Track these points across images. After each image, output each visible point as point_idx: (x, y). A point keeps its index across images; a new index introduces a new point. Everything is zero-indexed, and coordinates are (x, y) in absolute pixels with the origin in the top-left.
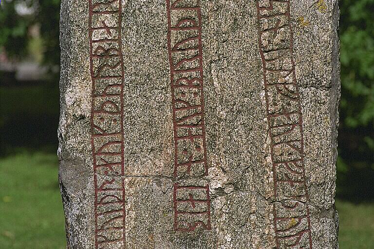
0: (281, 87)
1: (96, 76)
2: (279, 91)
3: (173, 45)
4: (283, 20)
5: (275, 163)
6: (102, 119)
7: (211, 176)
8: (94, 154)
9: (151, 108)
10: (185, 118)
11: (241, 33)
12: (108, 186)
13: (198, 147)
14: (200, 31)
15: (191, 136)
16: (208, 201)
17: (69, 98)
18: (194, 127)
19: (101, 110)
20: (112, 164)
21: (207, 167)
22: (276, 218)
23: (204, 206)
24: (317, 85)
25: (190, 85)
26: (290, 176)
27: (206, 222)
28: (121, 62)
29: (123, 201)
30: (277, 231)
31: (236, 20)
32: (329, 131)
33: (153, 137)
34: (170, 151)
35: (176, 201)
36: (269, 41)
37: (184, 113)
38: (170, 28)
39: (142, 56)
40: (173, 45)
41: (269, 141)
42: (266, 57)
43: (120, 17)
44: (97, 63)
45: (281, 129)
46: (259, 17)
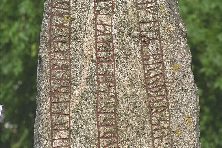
4: (166, 132)
11: (142, 140)
14: (117, 139)
31: (138, 132)
36: (159, 145)
43: (70, 132)
46: (152, 130)
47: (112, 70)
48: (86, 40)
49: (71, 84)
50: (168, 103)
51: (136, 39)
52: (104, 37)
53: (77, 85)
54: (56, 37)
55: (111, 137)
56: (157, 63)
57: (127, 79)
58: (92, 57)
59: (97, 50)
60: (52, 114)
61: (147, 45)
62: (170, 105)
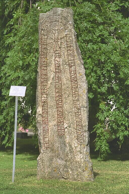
0: (77, 108)
2: (77, 108)
3: (57, 100)
4: (77, 95)
5: (76, 122)
6: (44, 114)
7: (64, 125)
8: (43, 121)
9: (53, 112)
10: (59, 114)
11: (69, 98)
12: (45, 127)
13: (62, 119)
14: (62, 97)
15: (61, 117)
16: (64, 130)
17: (38, 111)
18: (61, 115)
19: (44, 113)
20: (46, 123)
21: (64, 123)
22: (77, 133)
23: (63, 130)
24: (84, 107)
25: (60, 108)
26: (79, 124)
27: (64, 134)
28: (47, 103)
29: (48, 130)
30: (77, 135)
31: (68, 95)
32: (86, 116)
33: (54, 117)
34: (57, 120)
35: (58, 130)
37: (59, 113)
39: (51, 102)
40: (57, 100)
41: (75, 118)
42: (74, 102)
43: (47, 95)
44: (43, 104)
45: (77, 116)
46: (73, 95)
47: (60, 76)
48: (52, 66)
50: (78, 86)
51: (68, 66)
52: (58, 65)
53: (49, 80)
54: (43, 65)
55: (60, 97)
56: (74, 73)
57: (65, 78)
59: (56, 69)
60: (41, 89)
61: (71, 67)
62: (78, 87)
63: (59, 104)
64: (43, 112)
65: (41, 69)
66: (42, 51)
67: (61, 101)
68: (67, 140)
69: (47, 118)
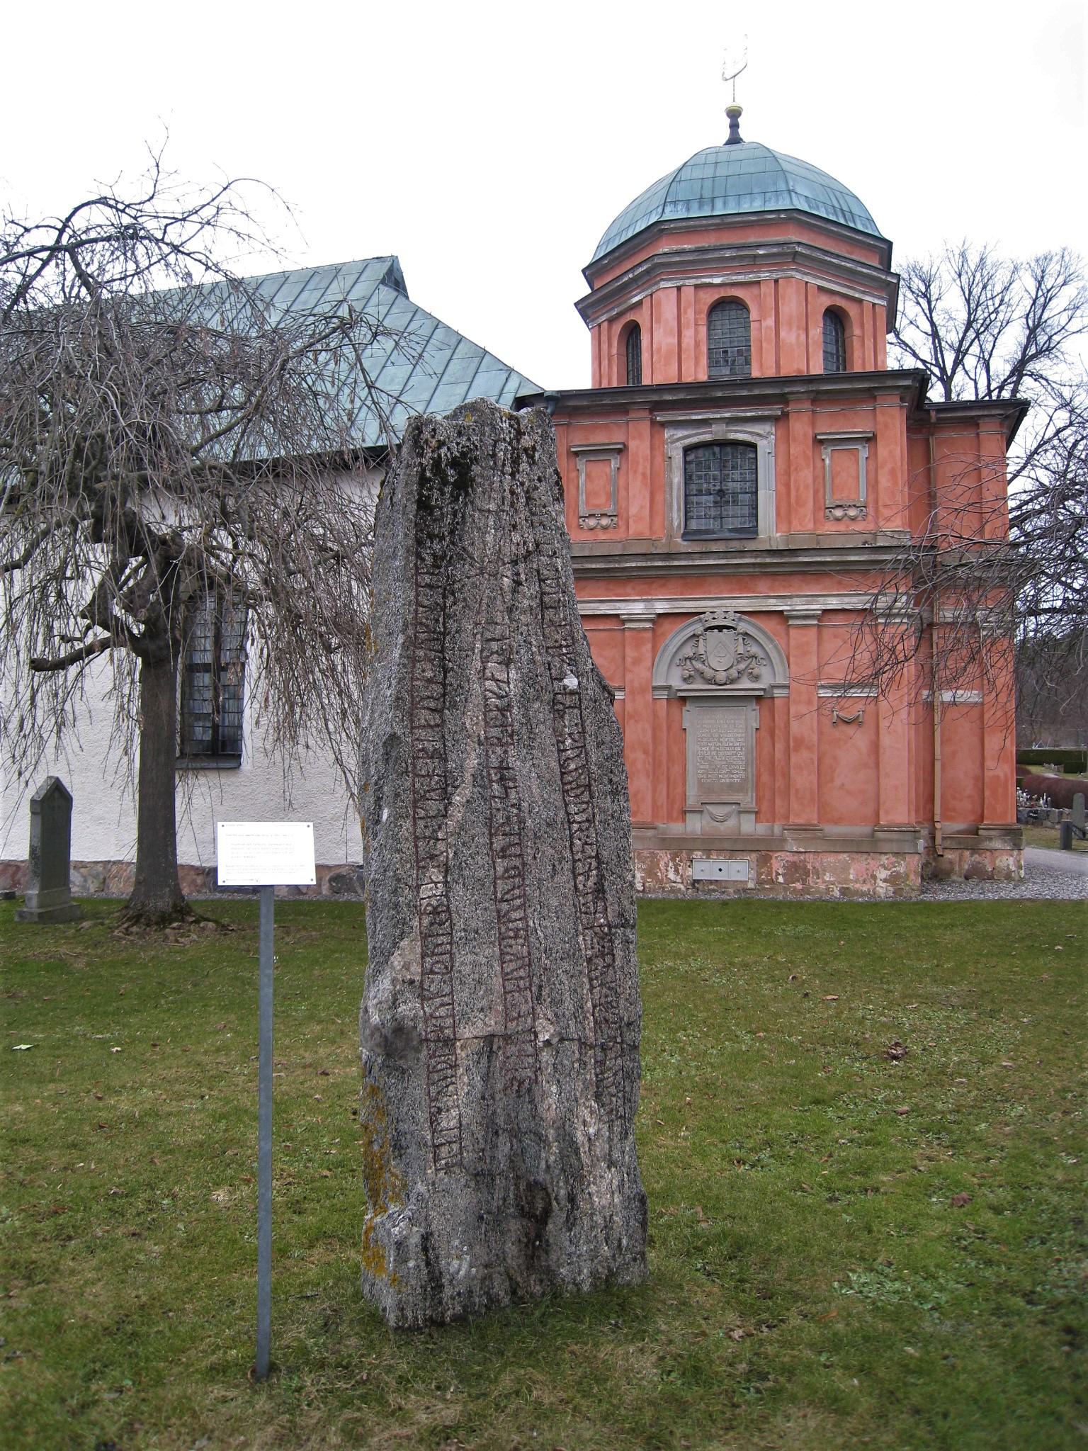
1: (425, 937)
3: (499, 895)
5: (594, 1007)
10: (512, 971)
13: (526, 1001)
15: (520, 990)
25: (516, 937)
28: (450, 918)
38: (496, 878)
40: (499, 895)
43: (447, 871)
46: (575, 861)
49: (447, 785)
52: (498, 702)
53: (457, 788)
54: (422, 699)
58: (479, 736)
60: (416, 838)
61: (562, 717)
62: (597, 818)
63: (514, 915)
64: (427, 966)
65: (412, 721)
66: (421, 624)
67: (518, 902)
68: (551, 1101)
69: (446, 999)
